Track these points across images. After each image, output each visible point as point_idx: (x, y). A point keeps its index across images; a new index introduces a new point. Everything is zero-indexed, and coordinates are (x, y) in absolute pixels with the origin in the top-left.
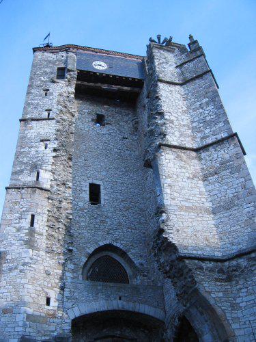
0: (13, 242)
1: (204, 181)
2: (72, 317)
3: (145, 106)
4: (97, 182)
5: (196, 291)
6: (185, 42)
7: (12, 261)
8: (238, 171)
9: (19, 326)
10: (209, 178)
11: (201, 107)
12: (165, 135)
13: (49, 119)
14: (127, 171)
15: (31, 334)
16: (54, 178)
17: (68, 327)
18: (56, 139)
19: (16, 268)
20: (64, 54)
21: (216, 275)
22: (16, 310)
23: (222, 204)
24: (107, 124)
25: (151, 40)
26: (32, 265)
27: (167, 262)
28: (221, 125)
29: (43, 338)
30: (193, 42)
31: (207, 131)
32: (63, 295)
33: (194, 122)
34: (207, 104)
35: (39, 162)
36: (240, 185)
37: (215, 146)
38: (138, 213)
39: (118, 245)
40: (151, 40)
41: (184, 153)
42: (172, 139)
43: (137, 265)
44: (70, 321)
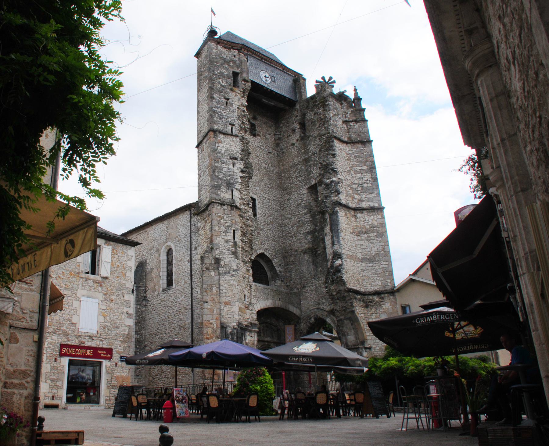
0: (224, 251)
1: (357, 236)
2: (257, 310)
3: (294, 131)
4: (255, 197)
6: (352, 97)
7: (225, 266)
10: (362, 235)
11: (360, 172)
12: (339, 194)
13: (232, 135)
14: (271, 188)
17: (255, 317)
18: (242, 160)
19: (229, 273)
20: (235, 52)
23: (368, 257)
24: (258, 135)
25: (323, 78)
27: (336, 290)
28: (374, 195)
30: (358, 99)
31: (364, 196)
32: (250, 293)
33: (355, 184)
34: (366, 172)
39: (267, 254)
40: (323, 78)
42: (343, 198)
43: (278, 272)
44: (256, 313)
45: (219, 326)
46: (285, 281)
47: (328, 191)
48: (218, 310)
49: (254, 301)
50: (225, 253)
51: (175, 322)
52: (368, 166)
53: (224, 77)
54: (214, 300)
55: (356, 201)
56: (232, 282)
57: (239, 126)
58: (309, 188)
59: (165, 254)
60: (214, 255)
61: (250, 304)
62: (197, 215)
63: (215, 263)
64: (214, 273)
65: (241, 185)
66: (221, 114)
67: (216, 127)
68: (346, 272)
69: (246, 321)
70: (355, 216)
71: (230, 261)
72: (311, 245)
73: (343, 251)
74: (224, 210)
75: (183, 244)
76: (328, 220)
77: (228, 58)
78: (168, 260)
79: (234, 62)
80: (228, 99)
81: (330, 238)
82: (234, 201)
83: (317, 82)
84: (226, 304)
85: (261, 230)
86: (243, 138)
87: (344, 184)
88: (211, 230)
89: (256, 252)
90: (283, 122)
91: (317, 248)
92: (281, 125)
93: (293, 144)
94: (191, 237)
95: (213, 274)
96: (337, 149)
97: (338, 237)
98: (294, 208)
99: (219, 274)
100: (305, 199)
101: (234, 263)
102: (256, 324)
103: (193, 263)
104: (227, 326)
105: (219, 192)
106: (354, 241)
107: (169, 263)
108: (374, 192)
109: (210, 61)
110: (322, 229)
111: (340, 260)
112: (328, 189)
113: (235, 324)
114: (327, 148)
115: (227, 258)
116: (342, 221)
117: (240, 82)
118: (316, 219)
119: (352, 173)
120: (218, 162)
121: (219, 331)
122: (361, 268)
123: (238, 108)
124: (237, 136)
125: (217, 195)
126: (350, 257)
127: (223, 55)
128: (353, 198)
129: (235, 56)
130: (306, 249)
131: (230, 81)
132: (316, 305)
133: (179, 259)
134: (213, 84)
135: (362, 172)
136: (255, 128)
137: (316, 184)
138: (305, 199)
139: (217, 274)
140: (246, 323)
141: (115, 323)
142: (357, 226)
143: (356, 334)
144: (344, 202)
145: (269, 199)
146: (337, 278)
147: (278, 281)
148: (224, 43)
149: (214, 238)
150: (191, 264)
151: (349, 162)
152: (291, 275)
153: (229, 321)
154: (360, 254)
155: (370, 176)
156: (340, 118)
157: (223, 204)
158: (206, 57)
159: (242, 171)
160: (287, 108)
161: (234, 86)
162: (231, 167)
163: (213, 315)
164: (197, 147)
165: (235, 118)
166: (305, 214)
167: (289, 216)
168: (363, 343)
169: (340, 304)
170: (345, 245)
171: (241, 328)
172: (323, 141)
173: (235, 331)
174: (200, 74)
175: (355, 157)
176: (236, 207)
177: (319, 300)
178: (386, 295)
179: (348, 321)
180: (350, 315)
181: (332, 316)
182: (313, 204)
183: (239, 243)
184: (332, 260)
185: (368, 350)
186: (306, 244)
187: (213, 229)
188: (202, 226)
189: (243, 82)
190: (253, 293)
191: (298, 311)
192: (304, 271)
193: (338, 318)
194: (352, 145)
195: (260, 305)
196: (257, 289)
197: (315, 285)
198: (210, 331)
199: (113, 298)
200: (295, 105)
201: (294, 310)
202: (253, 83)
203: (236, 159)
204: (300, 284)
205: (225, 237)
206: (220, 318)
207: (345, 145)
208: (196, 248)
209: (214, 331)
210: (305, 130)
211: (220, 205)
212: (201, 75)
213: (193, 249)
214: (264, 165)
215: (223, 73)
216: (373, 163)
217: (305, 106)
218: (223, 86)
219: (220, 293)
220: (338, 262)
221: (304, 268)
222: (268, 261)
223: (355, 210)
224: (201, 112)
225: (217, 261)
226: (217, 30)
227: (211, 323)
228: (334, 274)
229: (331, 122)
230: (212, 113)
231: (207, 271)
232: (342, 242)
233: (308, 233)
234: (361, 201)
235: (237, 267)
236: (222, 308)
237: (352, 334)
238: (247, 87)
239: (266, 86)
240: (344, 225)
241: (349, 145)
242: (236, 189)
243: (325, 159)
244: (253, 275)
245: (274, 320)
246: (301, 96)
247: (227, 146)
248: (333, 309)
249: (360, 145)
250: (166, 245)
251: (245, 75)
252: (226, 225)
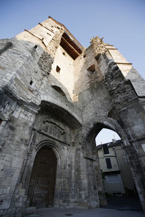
15: (14, 90)
17: (38, 103)
29: (21, 98)
58: (87, 69)
132: (94, 115)
197: (93, 103)
204: (82, 106)
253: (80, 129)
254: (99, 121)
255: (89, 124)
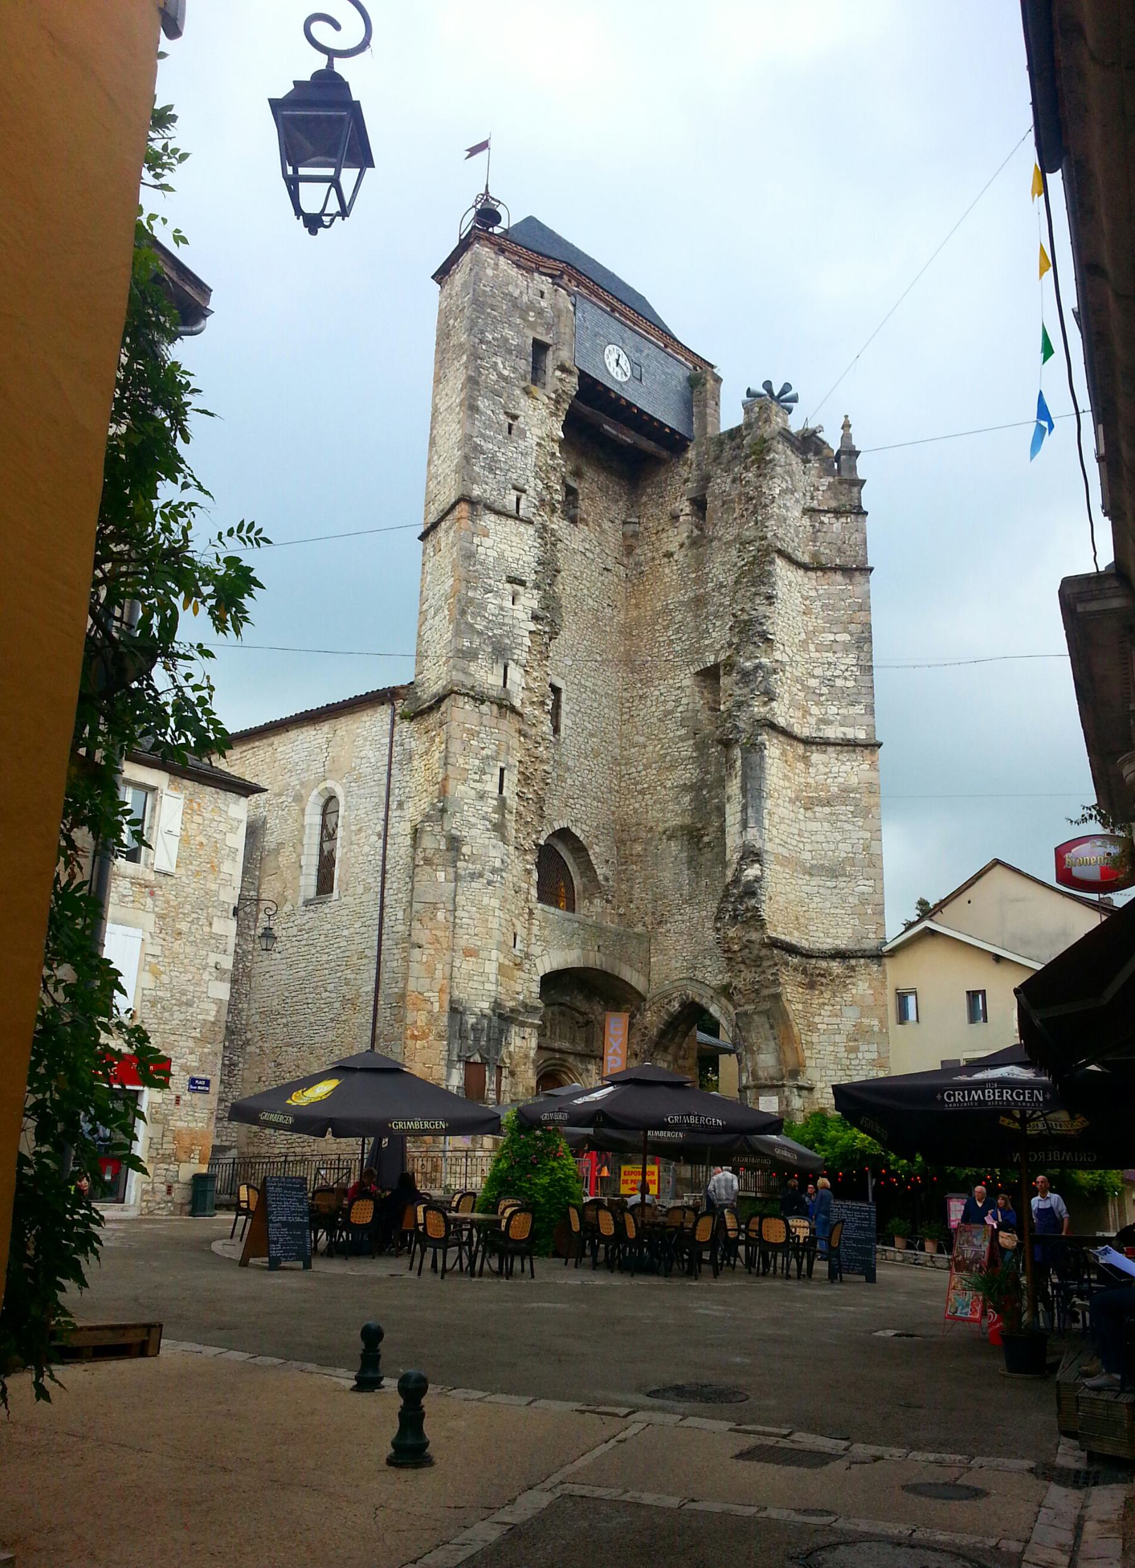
0: (473, 820)
1: (806, 809)
3: (675, 518)
4: (559, 683)
5: (777, 997)
7: (472, 858)
8: (865, 817)
9: (489, 981)
10: (817, 809)
11: (831, 647)
12: (772, 700)
16: (527, 684)
18: (537, 587)
19: (481, 876)
21: (800, 977)
22: (482, 954)
24: (582, 520)
25: (768, 385)
26: (504, 874)
28: (859, 709)
31: (834, 710)
32: (529, 929)
33: (814, 677)
34: (846, 651)
35: (507, 641)
36: (861, 841)
37: (839, 748)
38: (610, 769)
39: (578, 833)
40: (768, 385)
41: (791, 745)
42: (782, 712)
43: (601, 878)
44: (539, 978)
45: (447, 1008)
46: (615, 901)
47: (746, 691)
48: (447, 968)
49: (536, 950)
50: (474, 825)
51: (330, 987)
52: (851, 635)
53: (510, 352)
54: (439, 942)
55: (813, 721)
56: (486, 900)
57: (539, 494)
58: (697, 674)
59: (319, 810)
60: (446, 828)
61: (527, 956)
62: (412, 719)
63: (447, 849)
64: (443, 874)
65: (530, 652)
66: (494, 459)
67: (476, 491)
68: (770, 899)
69: (514, 999)
70: (805, 759)
71: (486, 847)
72: (688, 820)
73: (768, 846)
74: (481, 714)
75: (367, 791)
76: (739, 763)
77: (525, 298)
78: (324, 826)
79: (540, 313)
80: (515, 417)
81: (739, 808)
82: (508, 693)
83: (749, 393)
84: (469, 953)
85: (568, 769)
86: (544, 527)
87: (788, 675)
88: (445, 764)
89: (551, 824)
90: (649, 490)
91: (703, 828)
92: (644, 499)
93: (669, 555)
94: (389, 775)
95: (441, 876)
96: (780, 583)
97: (759, 810)
98: (654, 720)
99: (457, 878)
100: (684, 701)
101: (495, 852)
102: (537, 1008)
103: (389, 841)
104: (465, 1009)
105: (472, 667)
106: (796, 820)
107: (328, 834)
108: (860, 703)
109: (475, 301)
110: (721, 783)
111: (757, 866)
112: (747, 684)
113: (485, 1005)
114: (756, 575)
115: (479, 840)
116: (774, 770)
117: (549, 371)
118: (709, 755)
119: (812, 647)
120: (475, 589)
121: (444, 1020)
122: (808, 889)
123: (539, 444)
124: (532, 523)
125: (466, 673)
126: (785, 861)
127: (511, 288)
128: (807, 712)
129: (542, 295)
130: (675, 829)
131: (525, 366)
133: (353, 828)
134: (477, 368)
135: (836, 647)
136: (577, 499)
137: (716, 666)
138: (684, 701)
139: (451, 877)
140: (511, 1004)
141: (183, 993)
142: (808, 785)
143: (780, 1050)
144: (781, 721)
145: (594, 692)
146: (747, 910)
147: (597, 901)
148: (515, 253)
149: (451, 784)
150: (385, 841)
151: (805, 618)
152: (632, 887)
153: (472, 997)
154: (807, 856)
155: (854, 662)
156: (797, 501)
157: (479, 699)
158: (465, 285)
159: (535, 618)
160: (665, 454)
161: (534, 381)
162: (508, 604)
163: (433, 979)
164: (423, 537)
165: (528, 473)
166: (682, 739)
167: (642, 739)
168: (795, 1074)
169: (748, 975)
170: (774, 831)
171: (500, 1016)
172: (748, 557)
173: (485, 1022)
174: (444, 334)
175: (824, 607)
176: (513, 709)
177: (695, 958)
178: (862, 961)
179: (764, 1019)
180: (767, 1005)
181: (724, 1001)
182: (704, 716)
183: (513, 803)
184: (738, 863)
185: (804, 1093)
186: (676, 815)
187: (451, 761)
188: (422, 749)
189: (558, 373)
190: (535, 930)
191: (642, 979)
192: (666, 882)
193: (740, 1009)
194: (820, 573)
195: (549, 961)
196: (546, 920)
198: (421, 1018)
199: (183, 926)
200: (685, 448)
201: (633, 977)
202: (583, 376)
203: (522, 583)
204: (653, 913)
205: (478, 786)
206: (451, 987)
207: (801, 572)
208: (400, 805)
209: (433, 1019)
210: (704, 518)
211: (472, 702)
212: (448, 336)
213: (393, 806)
214: (590, 602)
215: (507, 340)
216: (867, 626)
217: (712, 454)
218: (505, 379)
219: (455, 924)
220: (752, 872)
221: (667, 876)
222: (579, 849)
223: (807, 742)
224: (440, 441)
225: (454, 843)
226: (500, 210)
227: (427, 1000)
228: (740, 902)
229: (774, 509)
230: (471, 451)
231: (428, 867)
232: (766, 822)
233: (686, 788)
234: (824, 721)
235: (503, 862)
236: (457, 963)
237: (771, 1050)
238: (567, 388)
239: (616, 388)
240: (775, 780)
241: (811, 574)
242: (517, 662)
243: (747, 607)
244: (540, 885)
245: (580, 997)
246: (704, 428)
247: (503, 546)
248: (730, 984)
249: (838, 577)
250: (322, 786)
251: (564, 355)
252: (484, 752)
253: (638, 1009)
254: (697, 1000)
255: (667, 997)
